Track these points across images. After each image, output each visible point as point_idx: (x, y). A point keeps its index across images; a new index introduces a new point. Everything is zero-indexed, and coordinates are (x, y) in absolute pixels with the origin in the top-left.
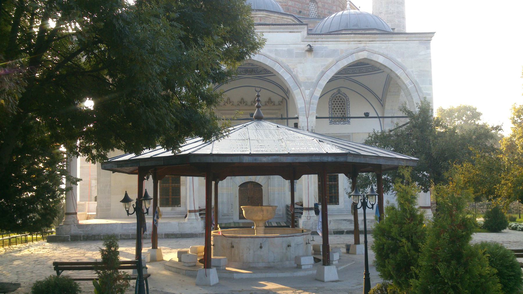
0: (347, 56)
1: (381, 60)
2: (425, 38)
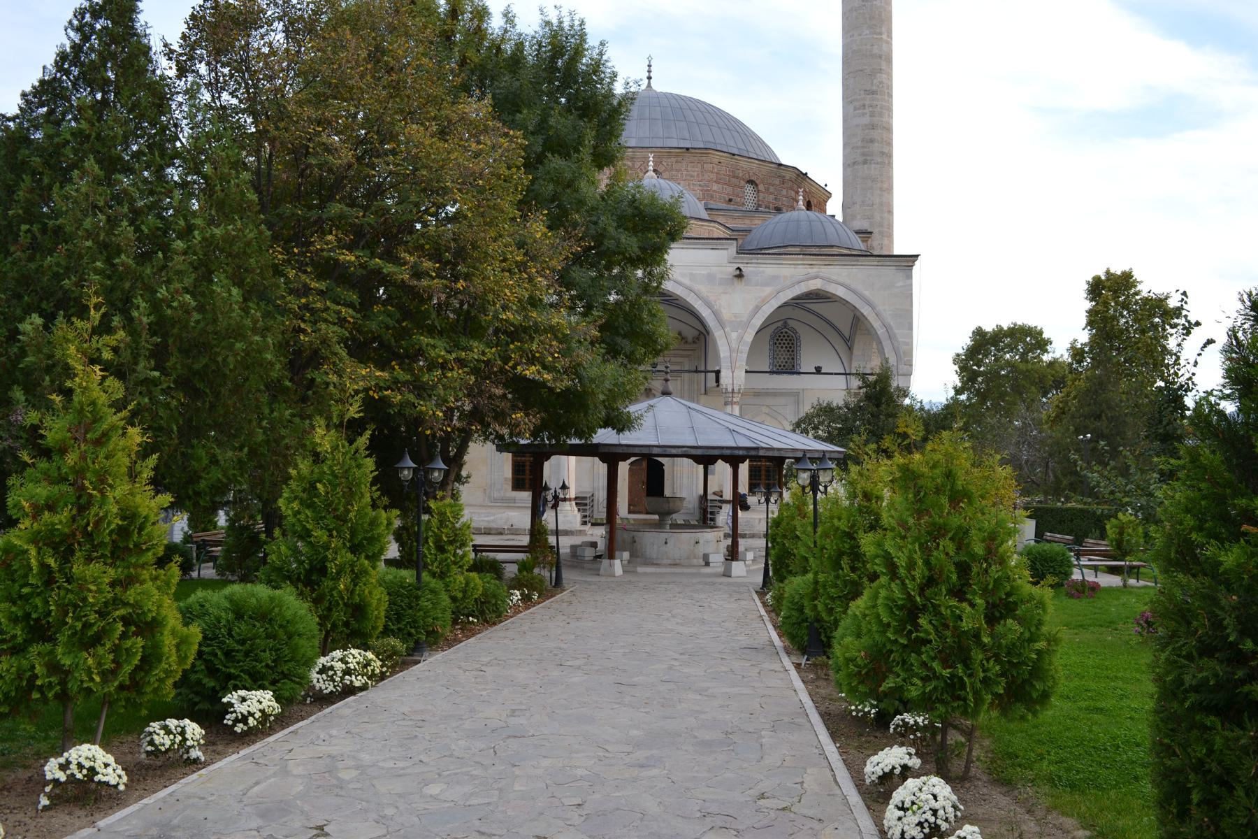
0: (793, 285)
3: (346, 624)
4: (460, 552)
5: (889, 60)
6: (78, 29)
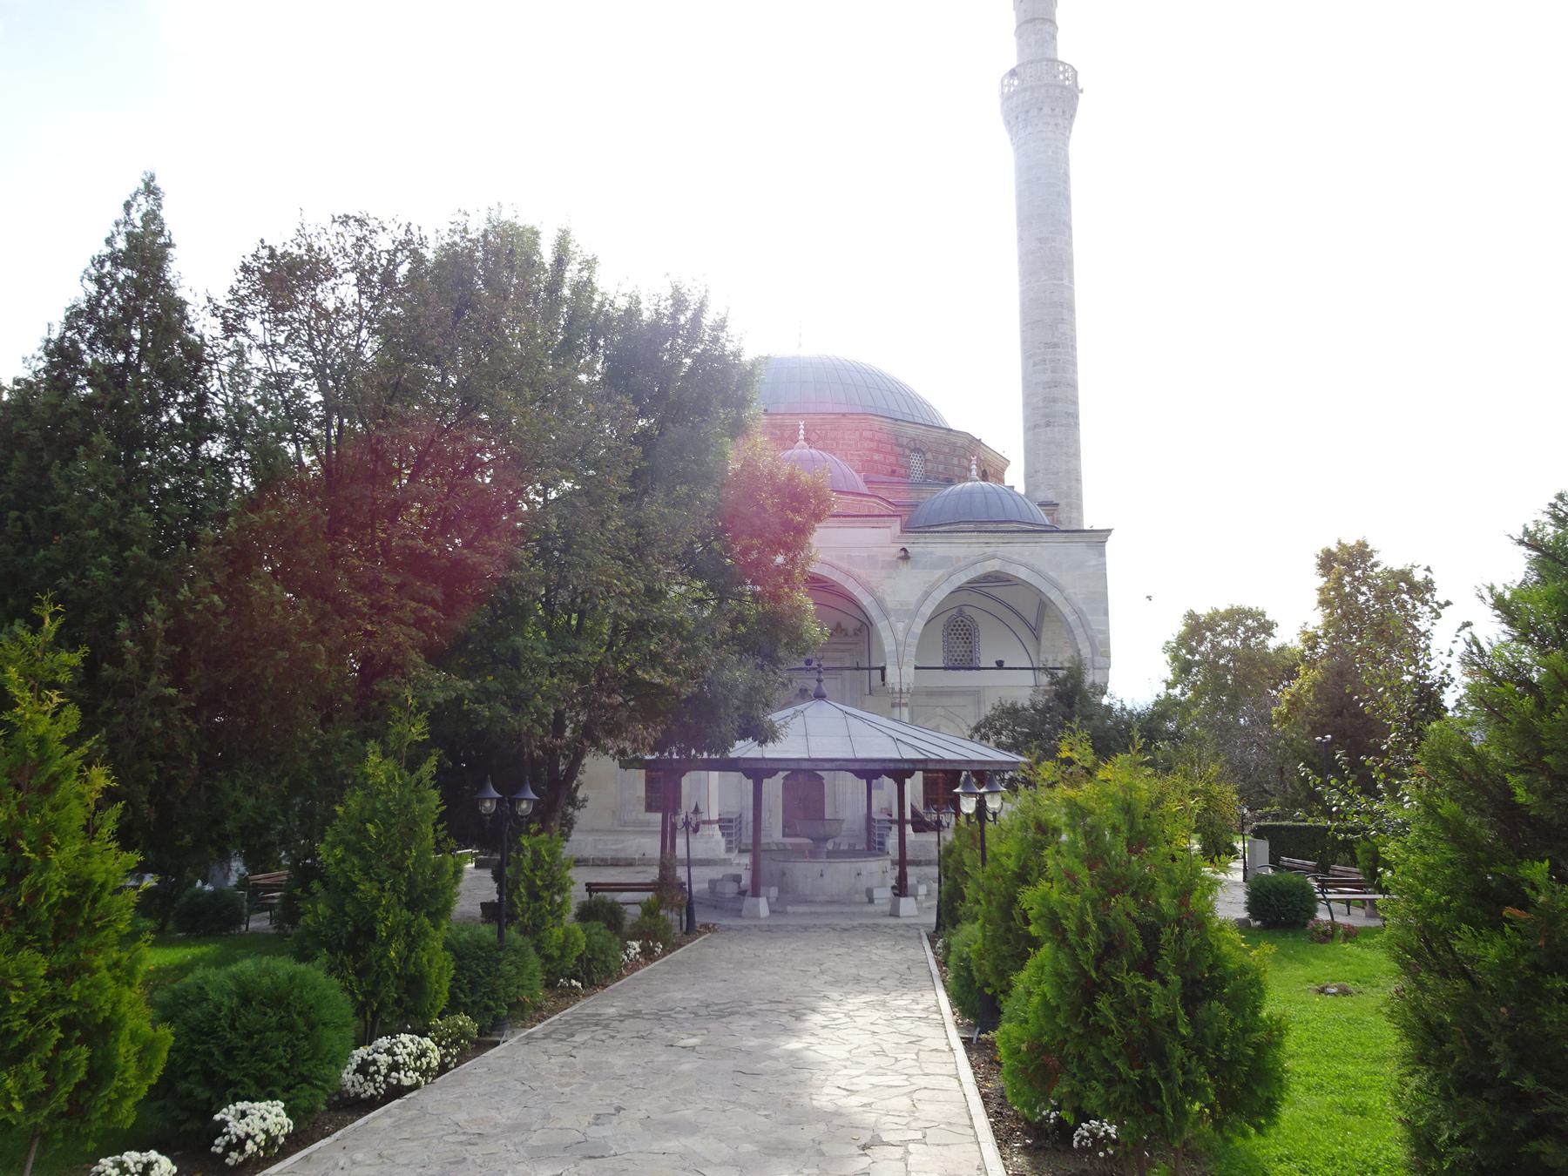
0: (967, 567)
1: (1023, 574)
2: (1099, 538)
3: (399, 1002)
4: (558, 899)
5: (1072, 309)
6: (99, 281)
